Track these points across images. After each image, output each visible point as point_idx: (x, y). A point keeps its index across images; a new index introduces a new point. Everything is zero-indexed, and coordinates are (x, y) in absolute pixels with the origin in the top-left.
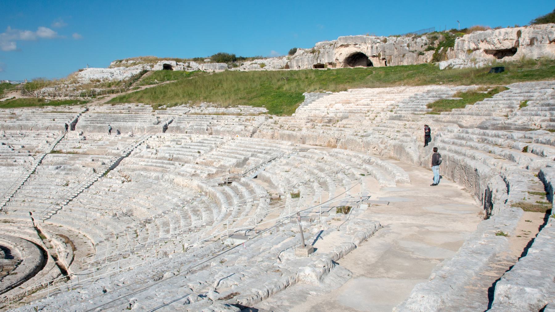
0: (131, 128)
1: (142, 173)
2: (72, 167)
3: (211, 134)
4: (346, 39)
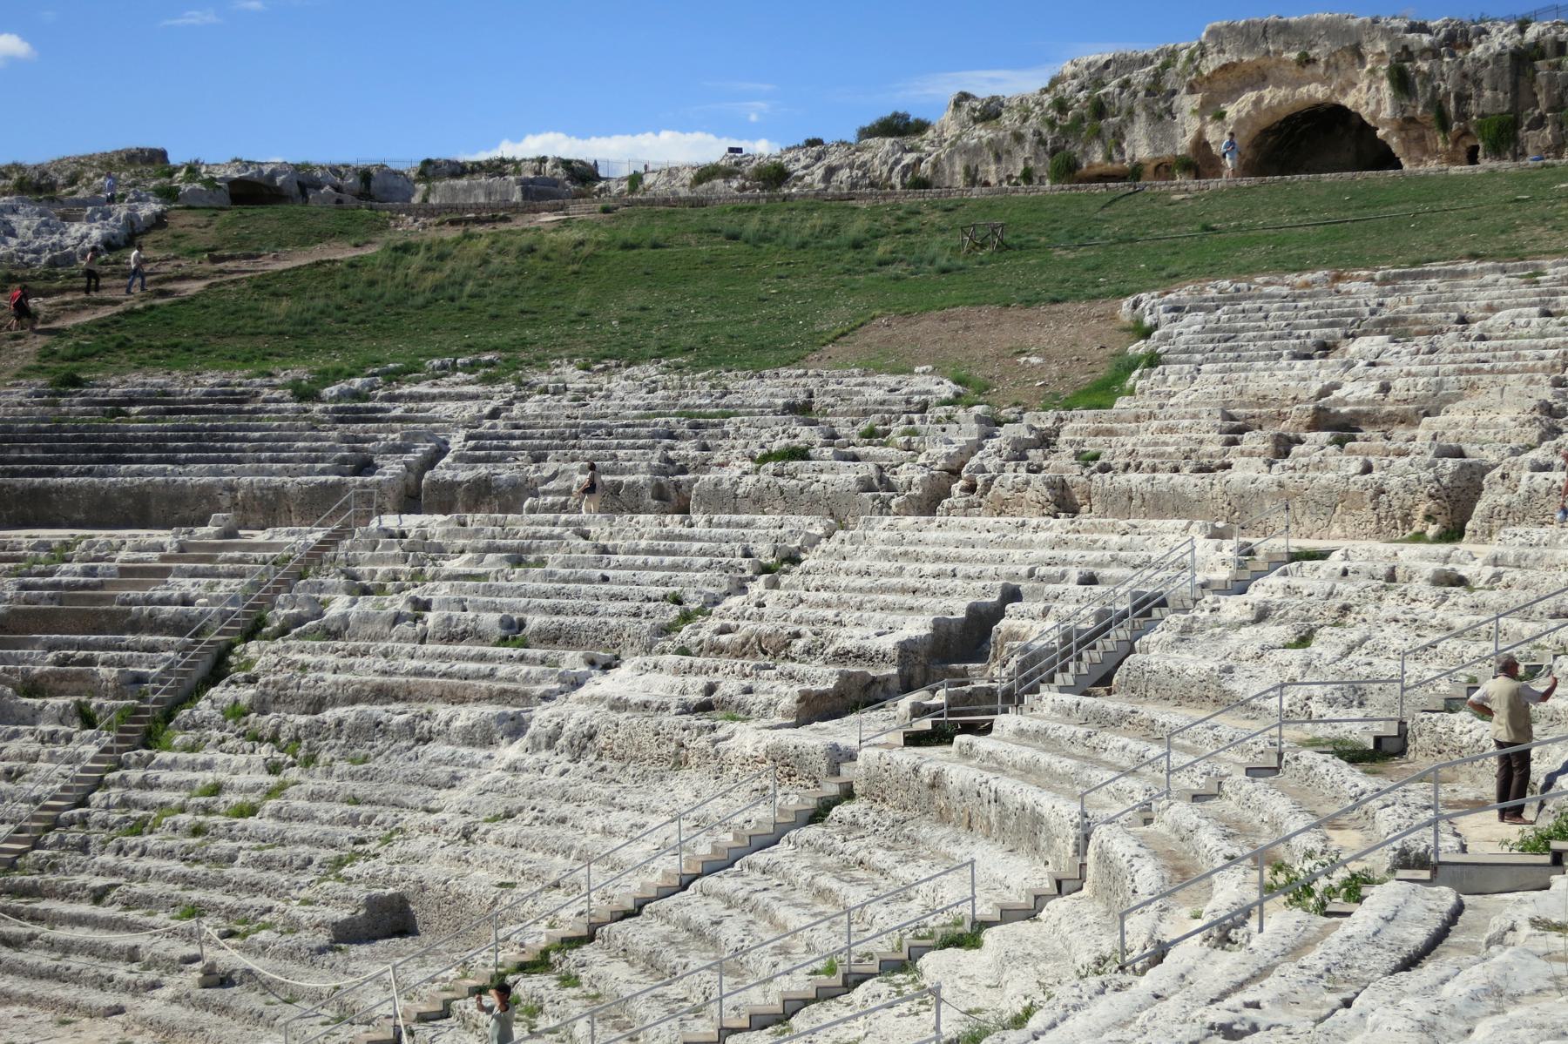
0: (206, 493)
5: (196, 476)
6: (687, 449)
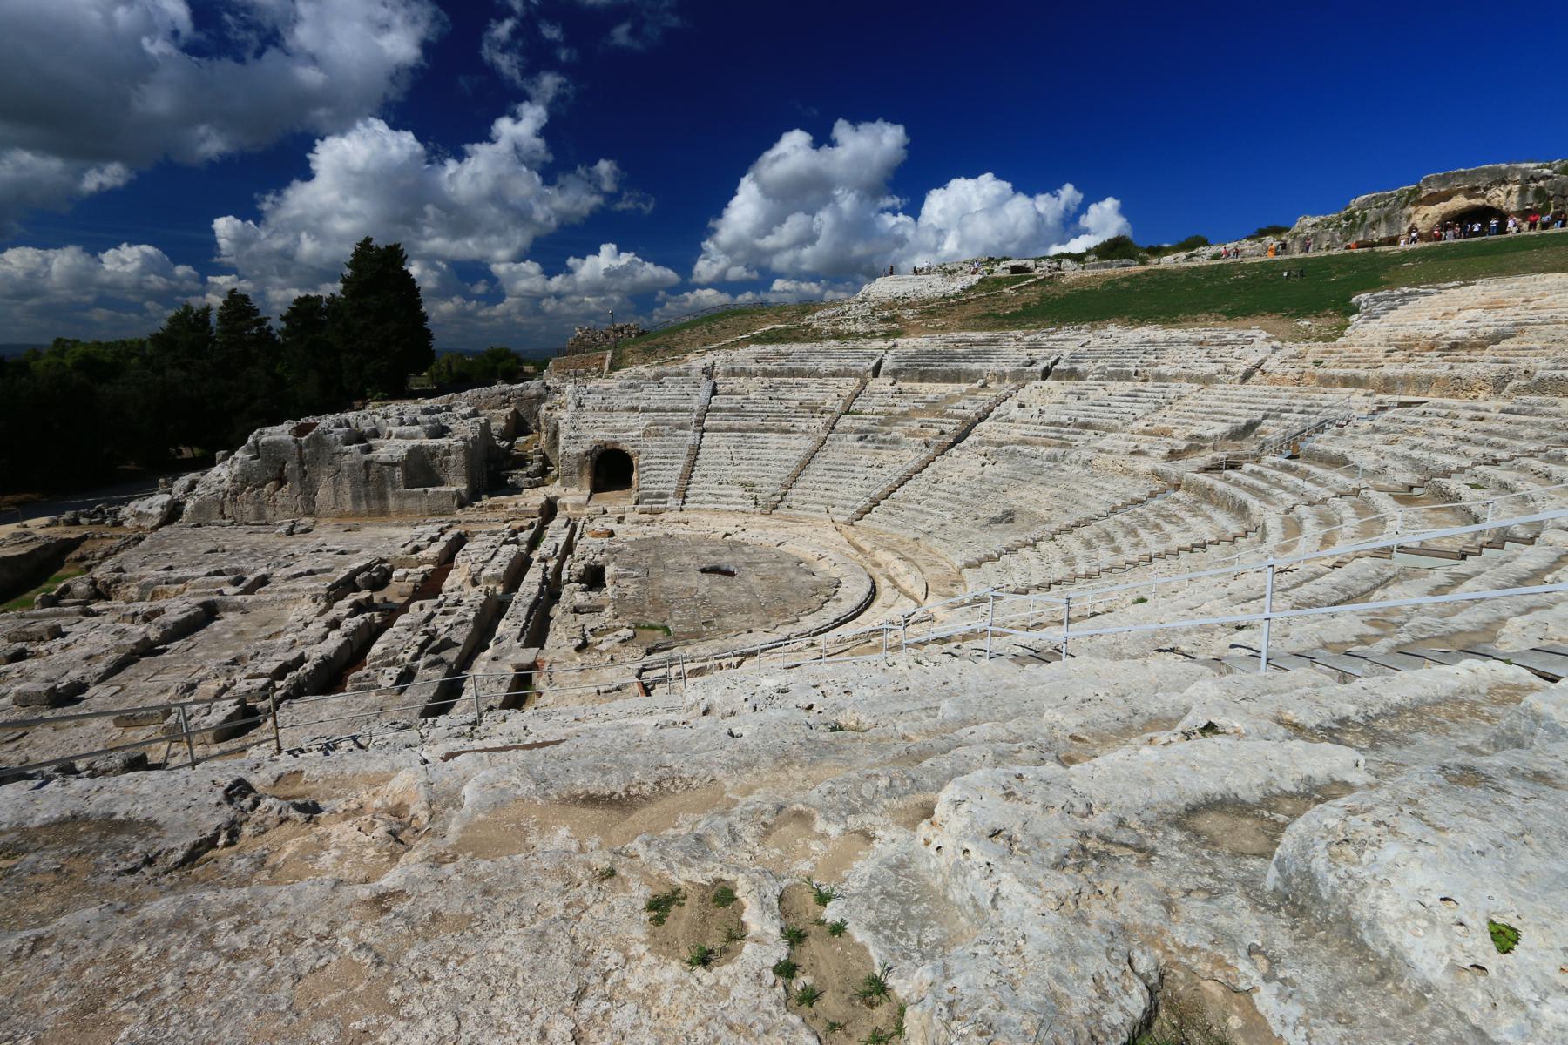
0: (979, 373)
1: (1019, 448)
2: (888, 438)
3: (1145, 381)
4: (1445, 180)
5: (976, 366)
6: (1152, 358)
